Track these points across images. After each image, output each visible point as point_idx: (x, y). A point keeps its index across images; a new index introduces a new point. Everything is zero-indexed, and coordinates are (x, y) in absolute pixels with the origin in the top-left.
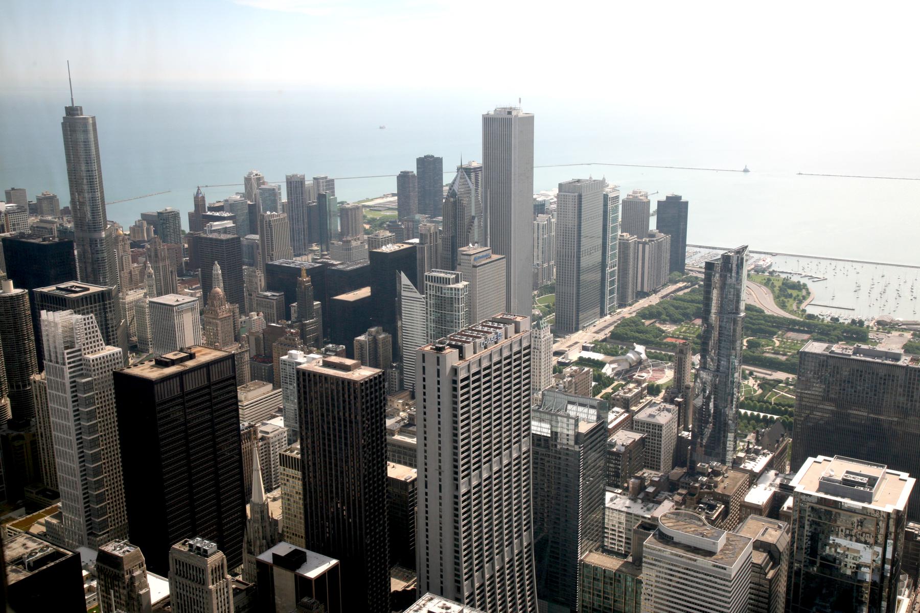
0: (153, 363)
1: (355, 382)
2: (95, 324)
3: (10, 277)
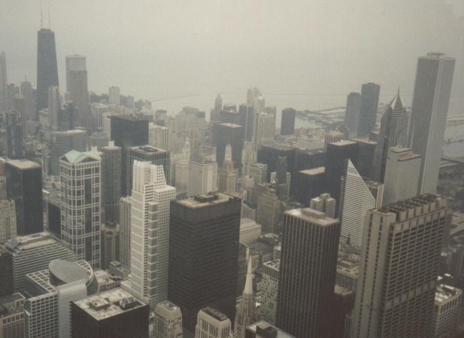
0: (193, 198)
1: (322, 228)
2: (163, 171)
3: (112, 139)
